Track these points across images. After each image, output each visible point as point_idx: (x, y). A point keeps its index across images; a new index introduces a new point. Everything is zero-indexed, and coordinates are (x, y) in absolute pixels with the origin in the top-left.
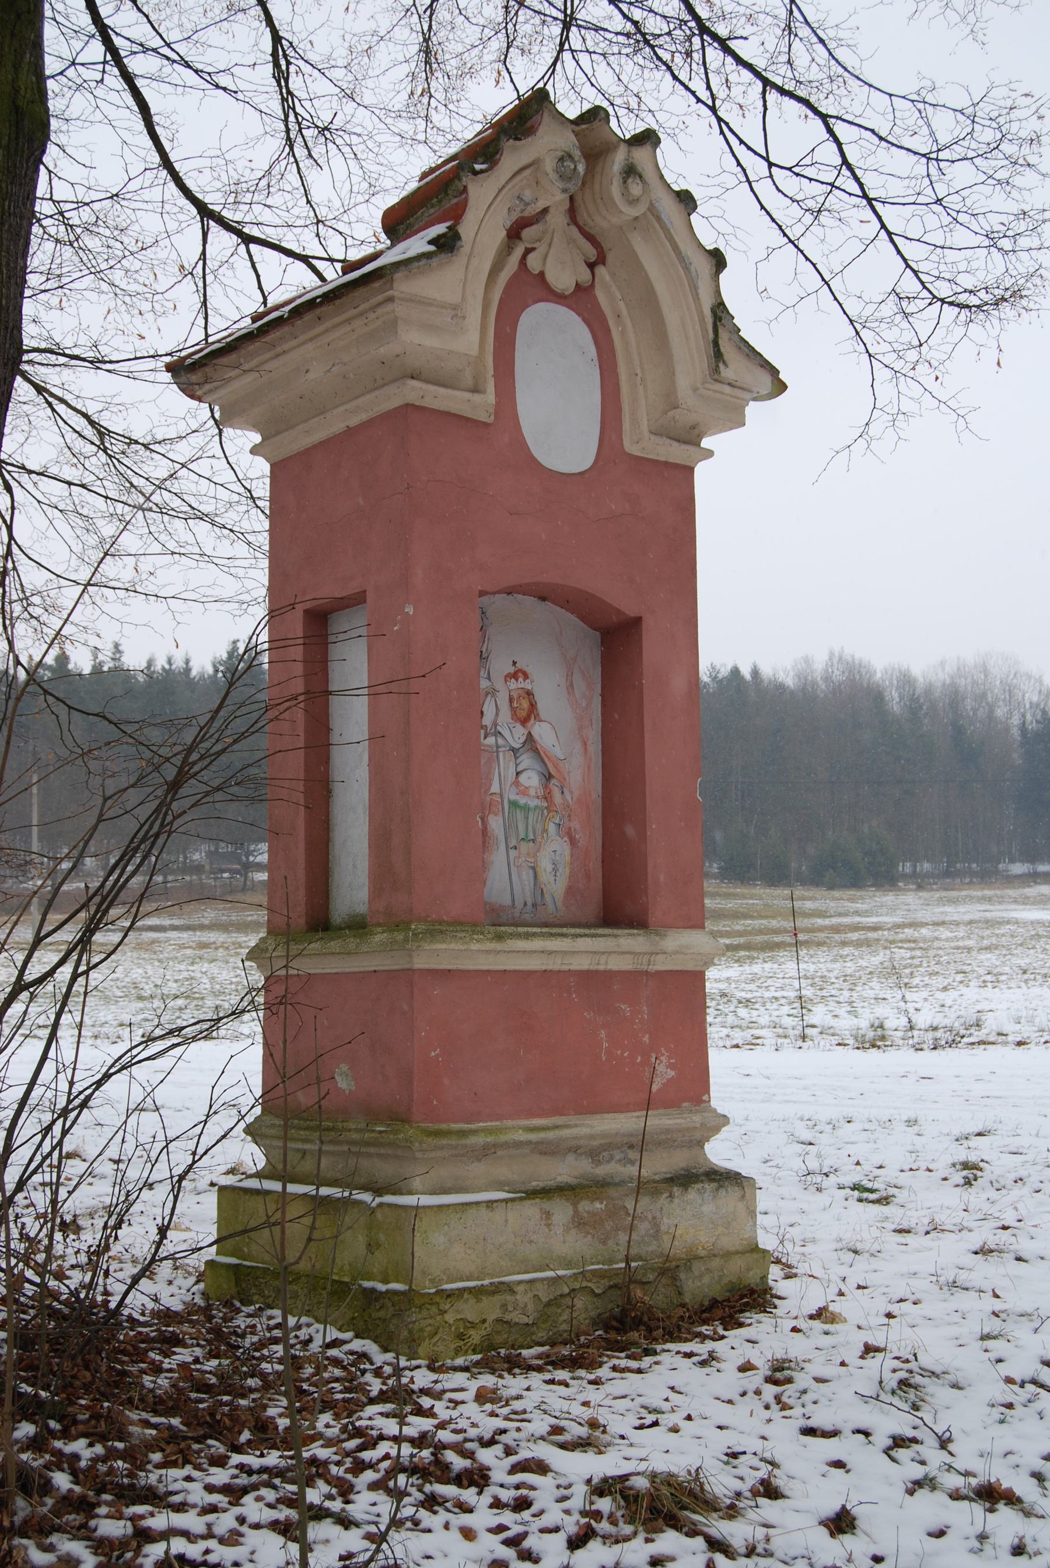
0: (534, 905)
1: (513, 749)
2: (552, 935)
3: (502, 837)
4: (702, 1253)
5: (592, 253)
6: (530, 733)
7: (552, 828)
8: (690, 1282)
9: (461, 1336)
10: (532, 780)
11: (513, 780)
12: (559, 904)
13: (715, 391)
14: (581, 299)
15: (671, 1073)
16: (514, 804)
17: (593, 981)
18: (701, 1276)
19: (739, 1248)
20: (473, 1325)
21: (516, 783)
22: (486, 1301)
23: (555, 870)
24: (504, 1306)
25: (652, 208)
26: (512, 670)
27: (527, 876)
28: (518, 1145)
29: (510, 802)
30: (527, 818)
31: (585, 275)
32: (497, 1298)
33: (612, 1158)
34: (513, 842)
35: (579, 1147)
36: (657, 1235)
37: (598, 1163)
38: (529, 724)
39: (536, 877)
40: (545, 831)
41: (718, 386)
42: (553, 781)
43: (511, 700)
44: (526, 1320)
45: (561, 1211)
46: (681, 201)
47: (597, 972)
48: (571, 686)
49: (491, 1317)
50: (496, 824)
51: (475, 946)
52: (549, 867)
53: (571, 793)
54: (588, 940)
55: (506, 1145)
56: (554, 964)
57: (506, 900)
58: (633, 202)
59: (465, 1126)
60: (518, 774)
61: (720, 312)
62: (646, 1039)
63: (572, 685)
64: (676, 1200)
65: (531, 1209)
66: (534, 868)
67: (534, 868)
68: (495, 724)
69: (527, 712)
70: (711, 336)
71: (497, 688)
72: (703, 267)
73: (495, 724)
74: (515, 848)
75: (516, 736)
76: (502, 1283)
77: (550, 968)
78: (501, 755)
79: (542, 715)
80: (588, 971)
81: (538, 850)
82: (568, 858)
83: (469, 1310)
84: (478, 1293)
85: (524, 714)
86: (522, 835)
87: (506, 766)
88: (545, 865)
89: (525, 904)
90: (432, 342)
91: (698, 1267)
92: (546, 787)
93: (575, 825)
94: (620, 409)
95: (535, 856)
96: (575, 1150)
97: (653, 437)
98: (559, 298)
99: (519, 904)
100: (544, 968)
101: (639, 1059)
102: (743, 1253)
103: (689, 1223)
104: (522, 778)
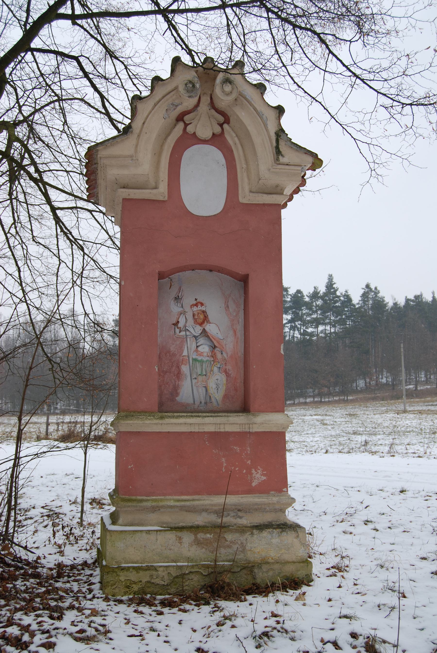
0: (206, 403)
1: (195, 337)
2: (192, 416)
3: (188, 374)
4: (270, 560)
5: (221, 119)
6: (204, 329)
7: (216, 369)
8: (261, 574)
9: (128, 587)
10: (205, 349)
11: (195, 350)
12: (220, 402)
13: (280, 169)
14: (217, 140)
15: (264, 478)
16: (195, 360)
18: (267, 572)
19: (295, 560)
20: (135, 583)
21: (196, 351)
22: (141, 573)
24: (151, 576)
25: (241, 94)
26: (195, 302)
27: (202, 391)
28: (171, 507)
29: (193, 359)
30: (202, 366)
31: (218, 130)
32: (148, 572)
33: (228, 515)
34: (195, 376)
35: (208, 510)
36: (244, 550)
38: (204, 325)
39: (207, 391)
40: (212, 370)
41: (280, 167)
42: (216, 349)
43: (194, 315)
44: (163, 583)
45: (188, 538)
46: (258, 88)
47: (220, 432)
48: (227, 307)
49: (144, 580)
50: (185, 369)
51: (147, 422)
52: (214, 386)
53: (227, 353)
54: (211, 418)
55: (163, 507)
57: (191, 401)
58: (228, 94)
59: (145, 498)
60: (197, 347)
61: (280, 133)
62: (249, 462)
63: (228, 307)
64: (255, 536)
65: (171, 536)
66: (206, 387)
67: (206, 387)
68: (185, 326)
69: (203, 319)
70: (274, 144)
71: (186, 311)
72: (271, 115)
73: (185, 326)
74: (196, 378)
76: (153, 566)
77: (193, 430)
78: (188, 339)
79: (211, 320)
80: (215, 432)
81: (208, 379)
82: (225, 382)
83: (133, 576)
84: (137, 569)
85: (201, 321)
86: (199, 373)
87: (191, 344)
88: (212, 385)
89: (201, 403)
90: (125, 172)
91: (265, 568)
92: (212, 352)
93: (229, 367)
94: (238, 185)
95: (206, 382)
96: (206, 510)
97: (251, 194)
99: (197, 403)
100: (190, 430)
101: (245, 471)
102: (294, 562)
103: (263, 547)
104: (200, 349)
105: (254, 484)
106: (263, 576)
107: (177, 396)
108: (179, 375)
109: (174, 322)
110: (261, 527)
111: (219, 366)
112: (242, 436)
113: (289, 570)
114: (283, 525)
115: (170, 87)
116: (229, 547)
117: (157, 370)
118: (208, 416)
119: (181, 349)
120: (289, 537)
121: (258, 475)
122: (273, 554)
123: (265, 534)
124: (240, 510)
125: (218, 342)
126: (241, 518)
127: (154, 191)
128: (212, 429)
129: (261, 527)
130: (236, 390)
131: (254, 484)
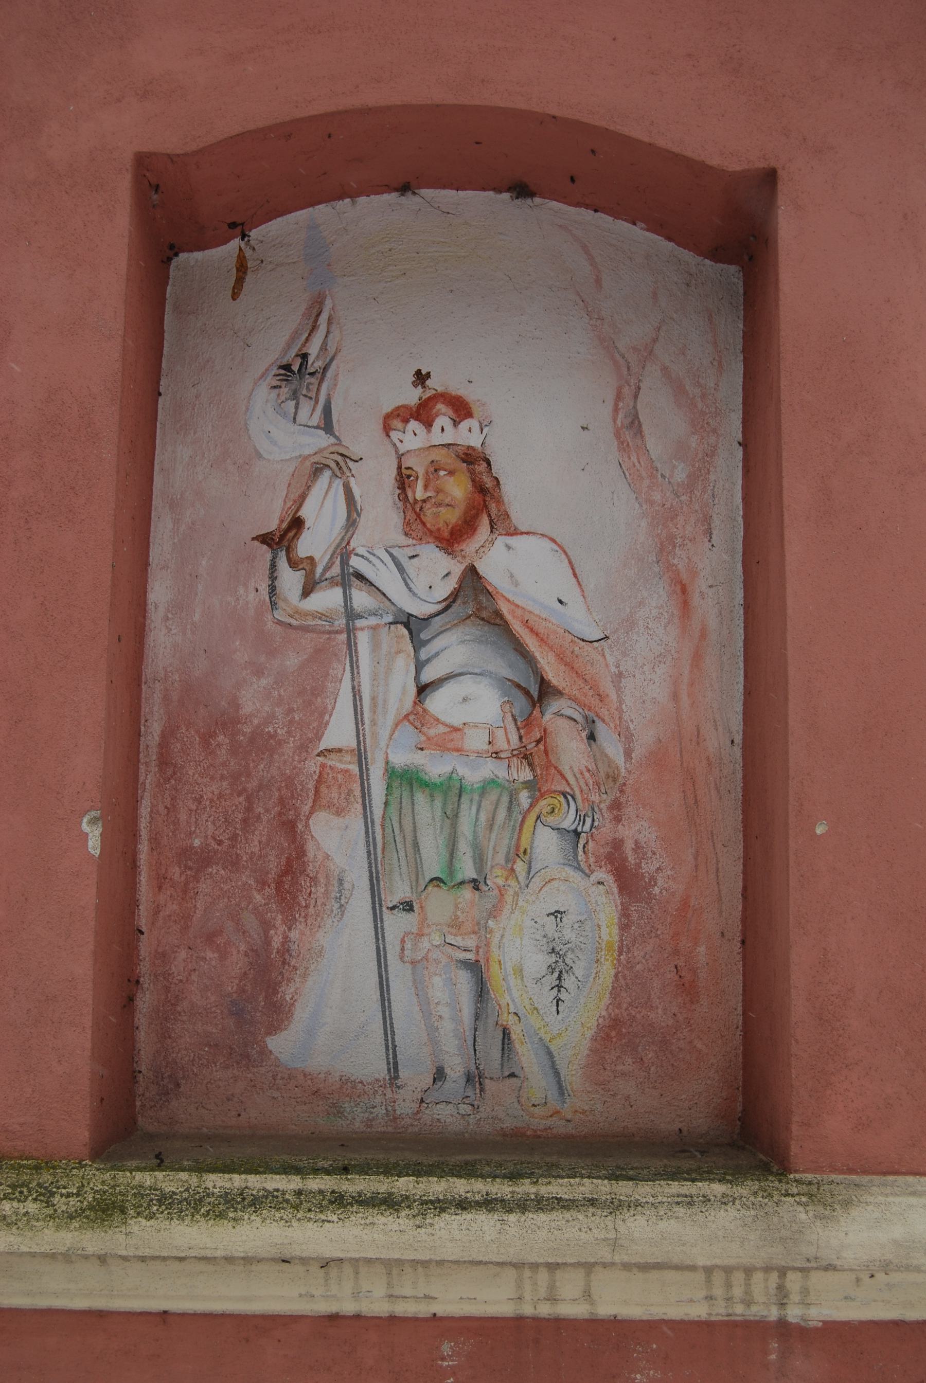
0: (475, 1078)
1: (408, 622)
2: (339, 1201)
3: (358, 878)
6: (472, 572)
7: (546, 845)
10: (476, 704)
11: (408, 711)
12: (572, 1075)
16: (405, 780)
21: (417, 716)
23: (559, 974)
26: (412, 396)
27: (451, 993)
30: (453, 818)
34: (399, 889)
38: (470, 547)
39: (482, 991)
40: (519, 852)
42: (555, 705)
43: (404, 480)
47: (558, 1323)
50: (335, 840)
52: (537, 962)
53: (627, 737)
54: (485, 1223)
60: (423, 690)
63: (635, 424)
66: (477, 970)
67: (477, 970)
68: (344, 553)
69: (464, 505)
71: (355, 450)
73: (344, 553)
74: (408, 907)
77: (348, 1307)
78: (363, 640)
79: (519, 514)
80: (518, 1321)
81: (494, 912)
82: (609, 932)
85: (452, 517)
86: (433, 866)
88: (519, 953)
89: (440, 1075)
92: (526, 724)
93: (638, 830)
95: (480, 929)
99: (415, 1077)
100: (323, 1307)
104: (440, 703)
107: (274, 1028)
108: (292, 880)
109: (272, 524)
111: (568, 822)
117: (94, 845)
118: (463, 1205)
125: (566, 660)
128: (495, 1299)
130: (687, 988)
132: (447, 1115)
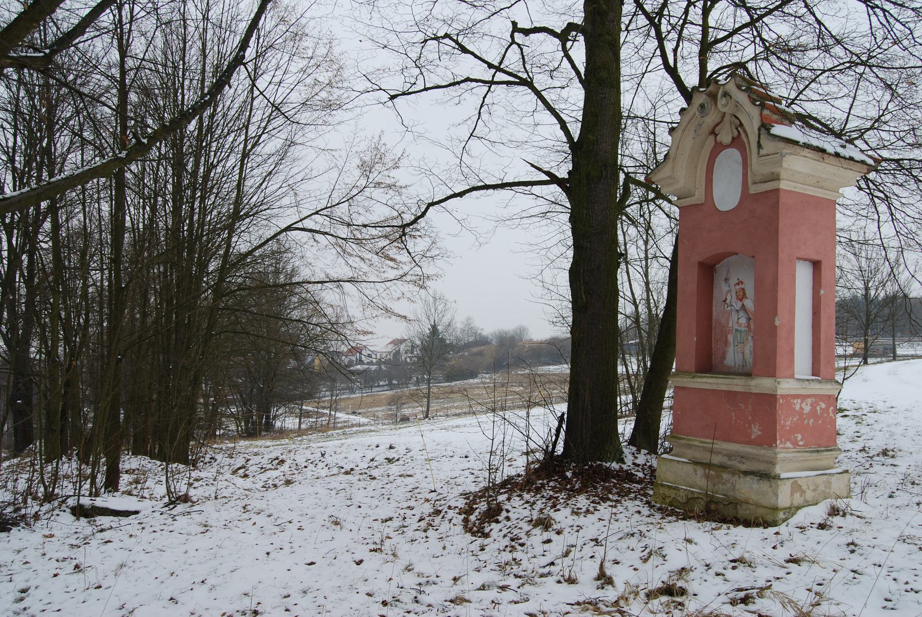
7: (750, 338)
10: (743, 321)
16: (737, 330)
17: (730, 395)
21: (738, 322)
22: (671, 491)
27: (740, 355)
36: (734, 489)
37: (730, 460)
45: (700, 471)
50: (730, 338)
55: (692, 445)
56: (715, 387)
57: (732, 364)
65: (690, 468)
69: (742, 296)
75: (738, 305)
83: (667, 492)
87: (734, 317)
98: (728, 146)
105: (753, 437)
106: (742, 512)
108: (726, 342)
110: (746, 473)
112: (746, 396)
113: (761, 511)
114: (765, 474)
115: (691, 113)
116: (724, 484)
119: (728, 321)
120: (764, 485)
121: (756, 430)
122: (754, 497)
123: (748, 478)
124: (743, 457)
126: (743, 463)
127: (692, 198)
128: (724, 388)
129: (746, 473)
131: (753, 437)
132: (740, 370)
